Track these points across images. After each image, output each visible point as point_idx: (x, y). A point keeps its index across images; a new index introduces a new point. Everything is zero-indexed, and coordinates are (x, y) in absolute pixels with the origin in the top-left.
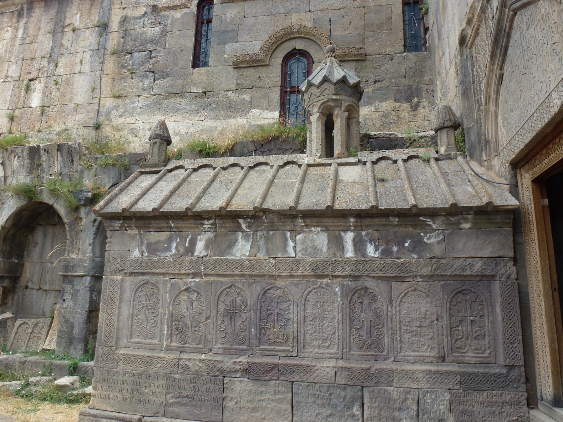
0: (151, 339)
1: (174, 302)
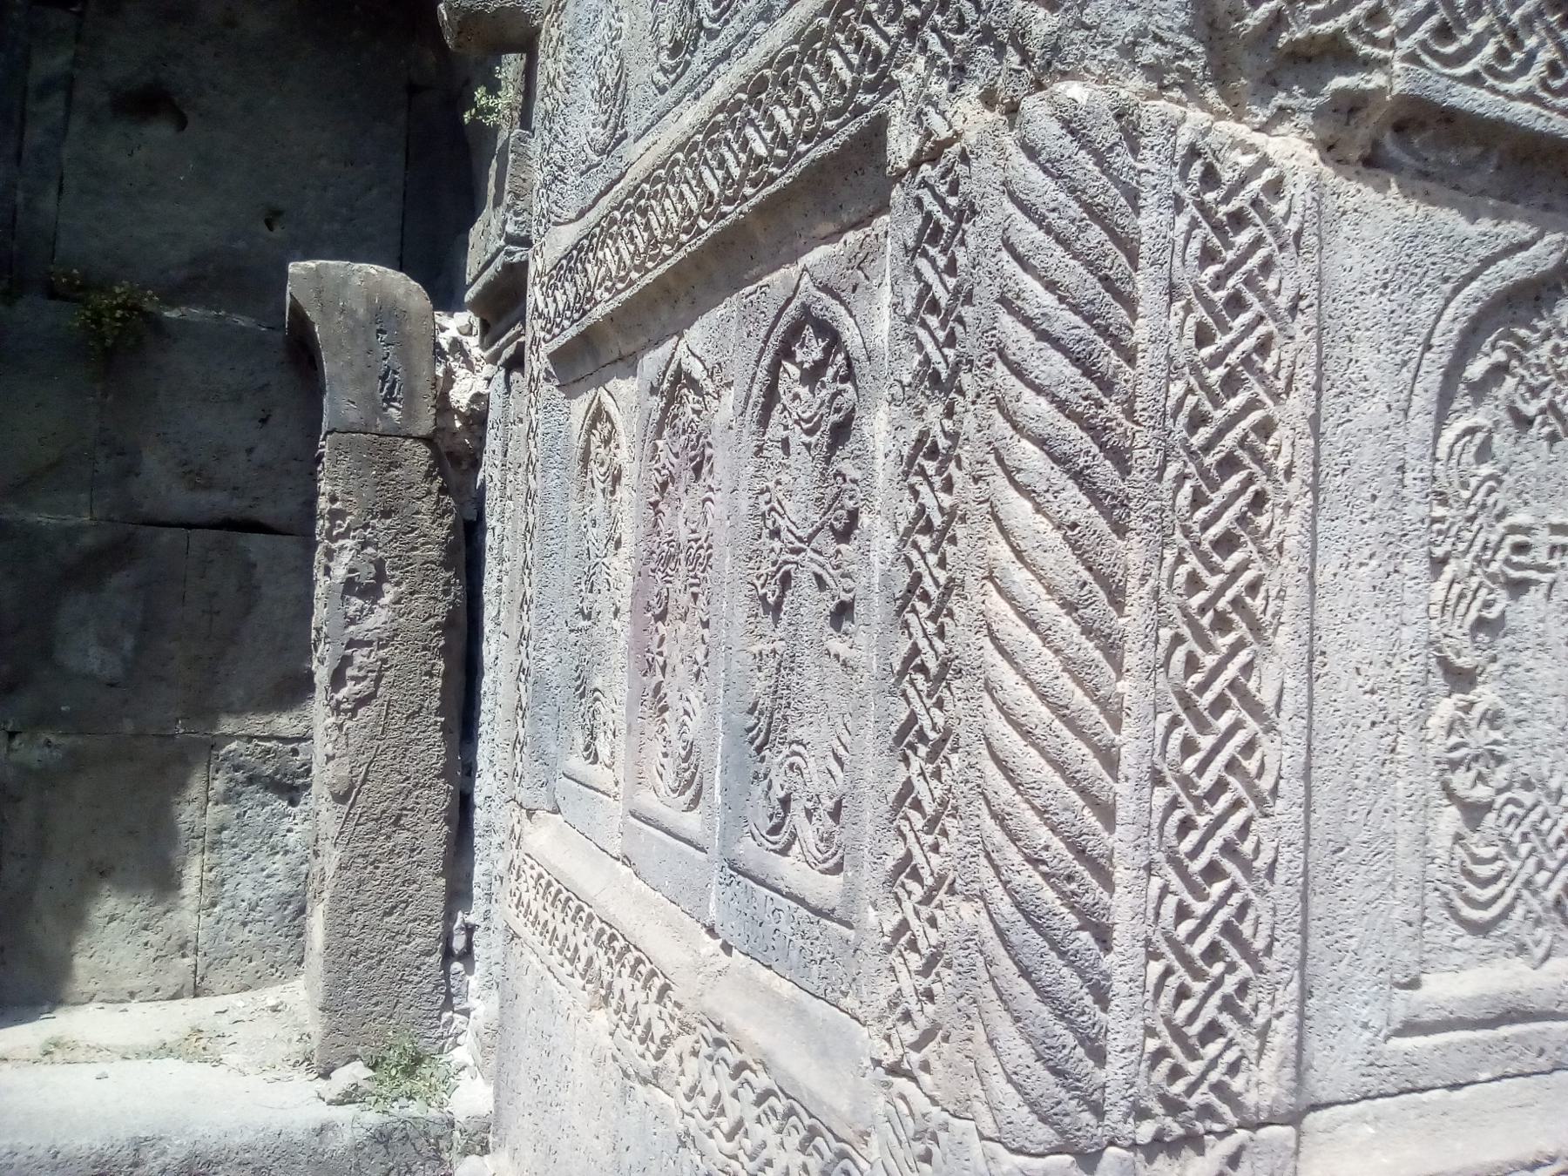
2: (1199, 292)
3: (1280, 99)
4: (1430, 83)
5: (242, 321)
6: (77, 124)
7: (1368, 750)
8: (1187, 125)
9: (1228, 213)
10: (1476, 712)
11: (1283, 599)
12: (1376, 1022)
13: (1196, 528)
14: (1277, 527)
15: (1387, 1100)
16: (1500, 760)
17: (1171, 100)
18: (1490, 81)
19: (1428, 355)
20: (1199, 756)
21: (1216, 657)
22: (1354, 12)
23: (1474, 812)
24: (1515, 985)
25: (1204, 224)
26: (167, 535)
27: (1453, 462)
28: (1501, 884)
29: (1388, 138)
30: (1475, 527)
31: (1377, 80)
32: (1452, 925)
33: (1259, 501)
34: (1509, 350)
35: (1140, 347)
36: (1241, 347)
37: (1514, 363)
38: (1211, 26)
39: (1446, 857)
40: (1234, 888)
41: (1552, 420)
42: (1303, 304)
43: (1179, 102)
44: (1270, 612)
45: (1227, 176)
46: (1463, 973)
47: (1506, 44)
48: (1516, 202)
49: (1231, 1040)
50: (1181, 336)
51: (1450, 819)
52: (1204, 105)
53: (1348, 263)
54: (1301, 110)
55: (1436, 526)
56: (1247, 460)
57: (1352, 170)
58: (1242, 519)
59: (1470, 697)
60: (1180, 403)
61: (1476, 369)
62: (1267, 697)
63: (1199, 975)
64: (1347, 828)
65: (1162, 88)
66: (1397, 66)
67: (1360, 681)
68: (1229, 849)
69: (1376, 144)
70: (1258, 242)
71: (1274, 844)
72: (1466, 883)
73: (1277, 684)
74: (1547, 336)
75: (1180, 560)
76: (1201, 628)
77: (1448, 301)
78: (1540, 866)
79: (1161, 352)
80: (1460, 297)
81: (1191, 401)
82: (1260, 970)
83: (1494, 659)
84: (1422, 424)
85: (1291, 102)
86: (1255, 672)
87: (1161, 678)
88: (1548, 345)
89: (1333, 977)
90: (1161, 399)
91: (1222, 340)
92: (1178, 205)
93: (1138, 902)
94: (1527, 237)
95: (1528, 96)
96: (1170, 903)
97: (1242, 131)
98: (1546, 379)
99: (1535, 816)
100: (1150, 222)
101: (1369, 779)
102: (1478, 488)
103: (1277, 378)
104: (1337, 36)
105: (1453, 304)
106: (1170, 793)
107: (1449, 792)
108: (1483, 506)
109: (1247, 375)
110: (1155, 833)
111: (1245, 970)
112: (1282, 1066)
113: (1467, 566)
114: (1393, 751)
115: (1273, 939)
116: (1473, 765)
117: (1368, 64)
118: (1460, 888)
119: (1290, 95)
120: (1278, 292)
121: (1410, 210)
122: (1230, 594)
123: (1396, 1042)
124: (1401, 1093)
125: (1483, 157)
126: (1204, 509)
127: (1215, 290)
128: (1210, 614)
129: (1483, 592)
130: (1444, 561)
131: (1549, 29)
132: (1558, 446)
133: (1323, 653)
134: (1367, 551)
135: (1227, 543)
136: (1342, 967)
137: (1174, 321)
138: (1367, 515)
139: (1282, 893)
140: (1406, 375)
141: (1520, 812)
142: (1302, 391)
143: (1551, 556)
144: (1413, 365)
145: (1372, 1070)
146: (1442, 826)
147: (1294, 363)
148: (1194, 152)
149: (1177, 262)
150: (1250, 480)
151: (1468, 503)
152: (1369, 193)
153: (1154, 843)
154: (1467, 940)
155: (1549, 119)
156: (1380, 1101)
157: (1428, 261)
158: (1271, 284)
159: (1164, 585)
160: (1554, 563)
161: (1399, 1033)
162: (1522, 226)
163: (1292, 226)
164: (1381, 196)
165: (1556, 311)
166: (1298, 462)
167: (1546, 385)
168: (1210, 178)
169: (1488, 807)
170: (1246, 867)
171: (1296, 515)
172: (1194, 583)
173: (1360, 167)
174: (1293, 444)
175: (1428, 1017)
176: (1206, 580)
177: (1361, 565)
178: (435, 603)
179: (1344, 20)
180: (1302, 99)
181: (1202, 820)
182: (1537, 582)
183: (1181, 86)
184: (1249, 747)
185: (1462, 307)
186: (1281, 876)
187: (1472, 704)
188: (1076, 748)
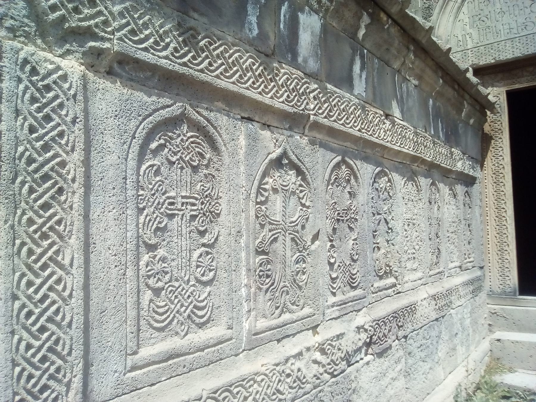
0: (200, 326)
1: (258, 193)
2: (30, 113)
3: (67, 46)
4: (128, 49)
7: (114, 276)
8: (24, 51)
9: (42, 86)
10: (157, 258)
11: (73, 226)
12: (120, 369)
13: (31, 201)
14: (69, 200)
15: (126, 395)
16: (167, 273)
17: (19, 42)
18: (152, 51)
19: (134, 140)
20: (35, 287)
21: (42, 249)
22: (96, 20)
23: (157, 292)
24: (173, 346)
25: (32, 88)
27: (146, 176)
28: (168, 313)
29: (115, 65)
30: (155, 197)
31: (107, 45)
32: (151, 330)
33: (60, 191)
34: (165, 140)
35: (3, 133)
36: (50, 135)
37: (168, 144)
38: (36, 14)
39: (147, 308)
40: (53, 334)
41: (181, 162)
42: (78, 120)
43: (23, 43)
44: (67, 230)
45: (42, 72)
46: (155, 346)
47: (158, 39)
48: (166, 92)
49: (54, 389)
50: (22, 129)
51: (148, 295)
52: (36, 45)
53: (100, 107)
54: (77, 52)
55: (140, 198)
56: (54, 175)
57: (102, 75)
58: (53, 198)
59: (155, 253)
60: (22, 154)
61: (154, 145)
62: (67, 262)
63: (37, 368)
64: (106, 304)
65: (15, 36)
66: (115, 41)
67: (110, 252)
68: (50, 320)
69: (111, 67)
70: (57, 97)
71: (71, 315)
72: (156, 315)
73: (70, 257)
74: (179, 136)
75: (24, 213)
76: (35, 239)
77: (141, 123)
78: (182, 306)
79: (12, 135)
80: (145, 122)
81: (27, 153)
82: (66, 361)
83: (164, 240)
84: (132, 163)
85: (72, 48)
86: (61, 253)
87: (16, 259)
88: (180, 139)
89: (101, 357)
90: (13, 152)
91: (41, 131)
93: (7, 346)
94: (170, 104)
95: (166, 58)
96: (23, 344)
97: (50, 56)
98: (179, 149)
99: (179, 290)
101: (114, 286)
102: (155, 184)
103: (67, 146)
104: (89, 27)
105: (143, 124)
106: (21, 302)
107: (147, 285)
108: (157, 190)
109: (54, 145)
110: (15, 319)
111: (59, 362)
112: (76, 394)
113: (152, 210)
114: (124, 274)
115: (71, 349)
116: (156, 276)
117: (103, 39)
118: (152, 317)
119: (71, 46)
120: (66, 115)
121: (125, 91)
122: (48, 225)
123: (129, 375)
124: (132, 391)
125: (153, 75)
126: (35, 194)
127: (38, 113)
128: (39, 233)
129: (158, 218)
130: (144, 209)
131: (174, 37)
132: (184, 171)
133: (94, 243)
134: (111, 207)
135: (46, 206)
136: (105, 353)
137: (19, 123)
138: (112, 194)
139: (76, 332)
140: (125, 147)
141: (174, 289)
142: (78, 151)
143: (182, 206)
144: (128, 143)
145: (119, 386)
146: (146, 298)
147: (74, 141)
148: (26, 61)
149: (19, 101)
150: (56, 183)
151: (152, 189)
152: (108, 84)
153: (14, 322)
154: (157, 334)
155: (174, 66)
156: (123, 396)
157: (133, 109)
158: (64, 112)
159: (16, 223)
160: (183, 208)
161: (130, 371)
162: (168, 100)
163: (72, 92)
164: (113, 85)
165: (182, 128)
166: (78, 177)
167: (179, 151)
168: (34, 71)
169: (163, 289)
170: (59, 325)
171: (77, 195)
172: (31, 222)
173: (105, 75)
174: (75, 170)
175: (140, 363)
176: (36, 221)
177: (109, 212)
179: (92, 22)
180: (77, 48)
181: (37, 311)
182: (178, 215)
183: (24, 36)
184: (59, 281)
185: (148, 124)
186: (74, 326)
187: (156, 255)
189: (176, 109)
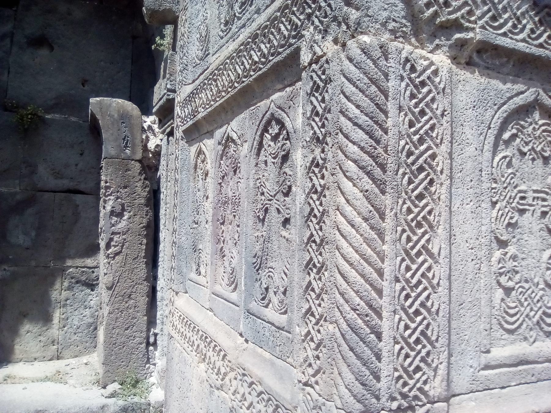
2: (410, 109)
3: (437, 41)
4: (489, 36)
5: (73, 119)
6: (15, 49)
7: (471, 269)
8: (405, 50)
9: (419, 81)
10: (508, 256)
11: (440, 216)
12: (475, 365)
13: (410, 191)
14: (438, 191)
15: (479, 393)
16: (517, 272)
17: (399, 42)
18: (510, 35)
19: (489, 131)
20: (412, 272)
21: (417, 237)
22: (463, 11)
23: (508, 291)
24: (523, 352)
25: (411, 85)
26: (47, 195)
27: (499, 168)
28: (518, 316)
29: (475, 56)
30: (507, 191)
31: (471, 35)
32: (501, 330)
33: (431, 182)
34: (517, 129)
35: (389, 128)
36: (424, 128)
37: (519, 133)
38: (413, 16)
39: (498, 307)
40: (425, 318)
41: (533, 153)
42: (446, 113)
43: (402, 43)
44: (436, 221)
45: (419, 68)
46: (505, 347)
47: (516, 22)
48: (519, 77)
49: (424, 372)
50: (403, 125)
51: (500, 293)
52: (410, 44)
53: (461, 99)
54: (445, 46)
55: (493, 191)
56: (427, 168)
57: (463, 66)
58: (426, 188)
59: (506, 250)
60: (404, 148)
61: (506, 136)
62: (435, 251)
63: (412, 349)
64: (464, 297)
65: (396, 37)
66: (478, 30)
67: (468, 245)
68: (423, 305)
69: (471, 57)
70: (430, 92)
71: (438, 303)
72: (506, 316)
73: (439, 246)
74: (531, 124)
75: (404, 203)
76: (412, 226)
77: (496, 112)
78: (532, 310)
79: (397, 130)
80: (500, 111)
81: (407, 147)
82: (434, 347)
83: (514, 237)
84: (488, 155)
85: (441, 42)
86: (431, 242)
87: (398, 244)
88: (531, 127)
89: (459, 349)
90: (397, 146)
91: (418, 126)
92: (402, 79)
93: (391, 324)
94: (523, 89)
95: (523, 40)
96: (402, 324)
97: (424, 53)
98: (530, 139)
99: (529, 292)
100: (392, 84)
101: (471, 280)
102: (508, 177)
103: (437, 139)
104: (456, 19)
105: (498, 113)
106: (402, 285)
107: (499, 283)
108: (510, 183)
109: (427, 138)
110: (396, 299)
111: (429, 347)
112: (442, 381)
113: (504, 204)
114: (479, 269)
115: (438, 336)
116: (508, 274)
117: (467, 29)
118: (503, 317)
119: (441, 40)
120: (437, 109)
121: (483, 80)
122: (422, 215)
123: (482, 372)
124: (484, 390)
125: (508, 62)
126: (412, 185)
127: (415, 108)
128: (415, 222)
129: (510, 213)
130: (496, 203)
131: (531, 17)
132: (535, 162)
133: (455, 235)
134: (469, 200)
135: (420, 197)
136: (463, 346)
137: (401, 119)
138: (469, 187)
139: (441, 320)
140: (482, 138)
141: (524, 290)
142: (446, 143)
143: (533, 201)
144: (484, 134)
145: (474, 382)
146: (497, 296)
147: (443, 133)
148: (407, 60)
149: (402, 98)
150: (428, 175)
151: (504, 182)
152: (468, 75)
153: (396, 303)
154: (506, 336)
155: (531, 48)
156: (477, 393)
157: (489, 98)
158: (435, 106)
159: (398, 211)
160: (534, 203)
161: (483, 369)
162: (522, 86)
163: (442, 86)
164: (472, 75)
165: (534, 115)
166: (445, 168)
167: (531, 141)
168: (413, 69)
169: (513, 289)
170: (429, 311)
171: (444, 187)
172: (409, 211)
173: (465, 66)
174: (443, 162)
175: (493, 363)
176: (413, 210)
177: (467, 204)
178: (142, 219)
179: (459, 14)
180: (444, 42)
181: (413, 295)
182: (529, 210)
183: (402, 37)
184: (429, 269)
185: (501, 114)
186: (441, 314)
187: (507, 253)
188: (369, 270)
189: (529, 96)
